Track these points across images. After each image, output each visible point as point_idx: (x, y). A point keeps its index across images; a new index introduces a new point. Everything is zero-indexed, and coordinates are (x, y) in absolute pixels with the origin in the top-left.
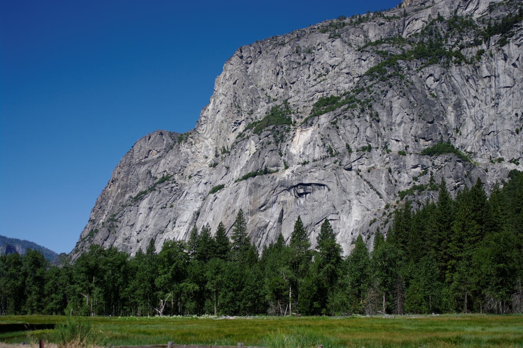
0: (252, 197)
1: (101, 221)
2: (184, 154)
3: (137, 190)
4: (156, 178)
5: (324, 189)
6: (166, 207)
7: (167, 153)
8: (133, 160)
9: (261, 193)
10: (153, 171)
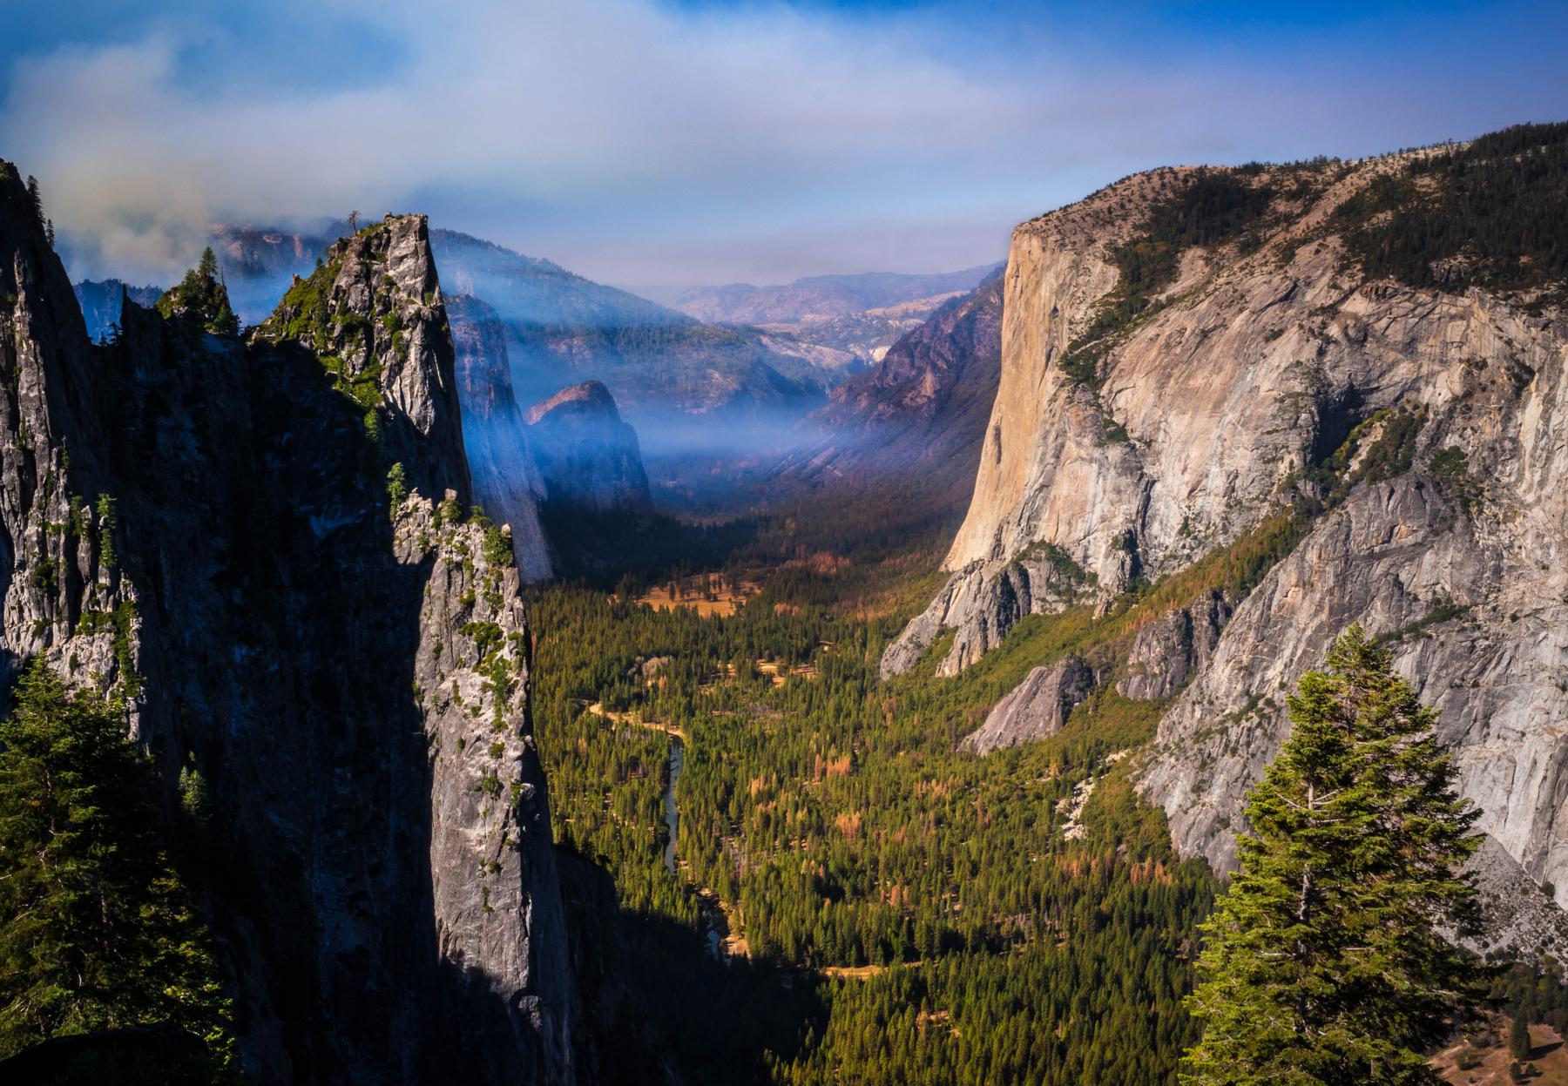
3: (1369, 620)
8: (1353, 546)
10: (1403, 577)
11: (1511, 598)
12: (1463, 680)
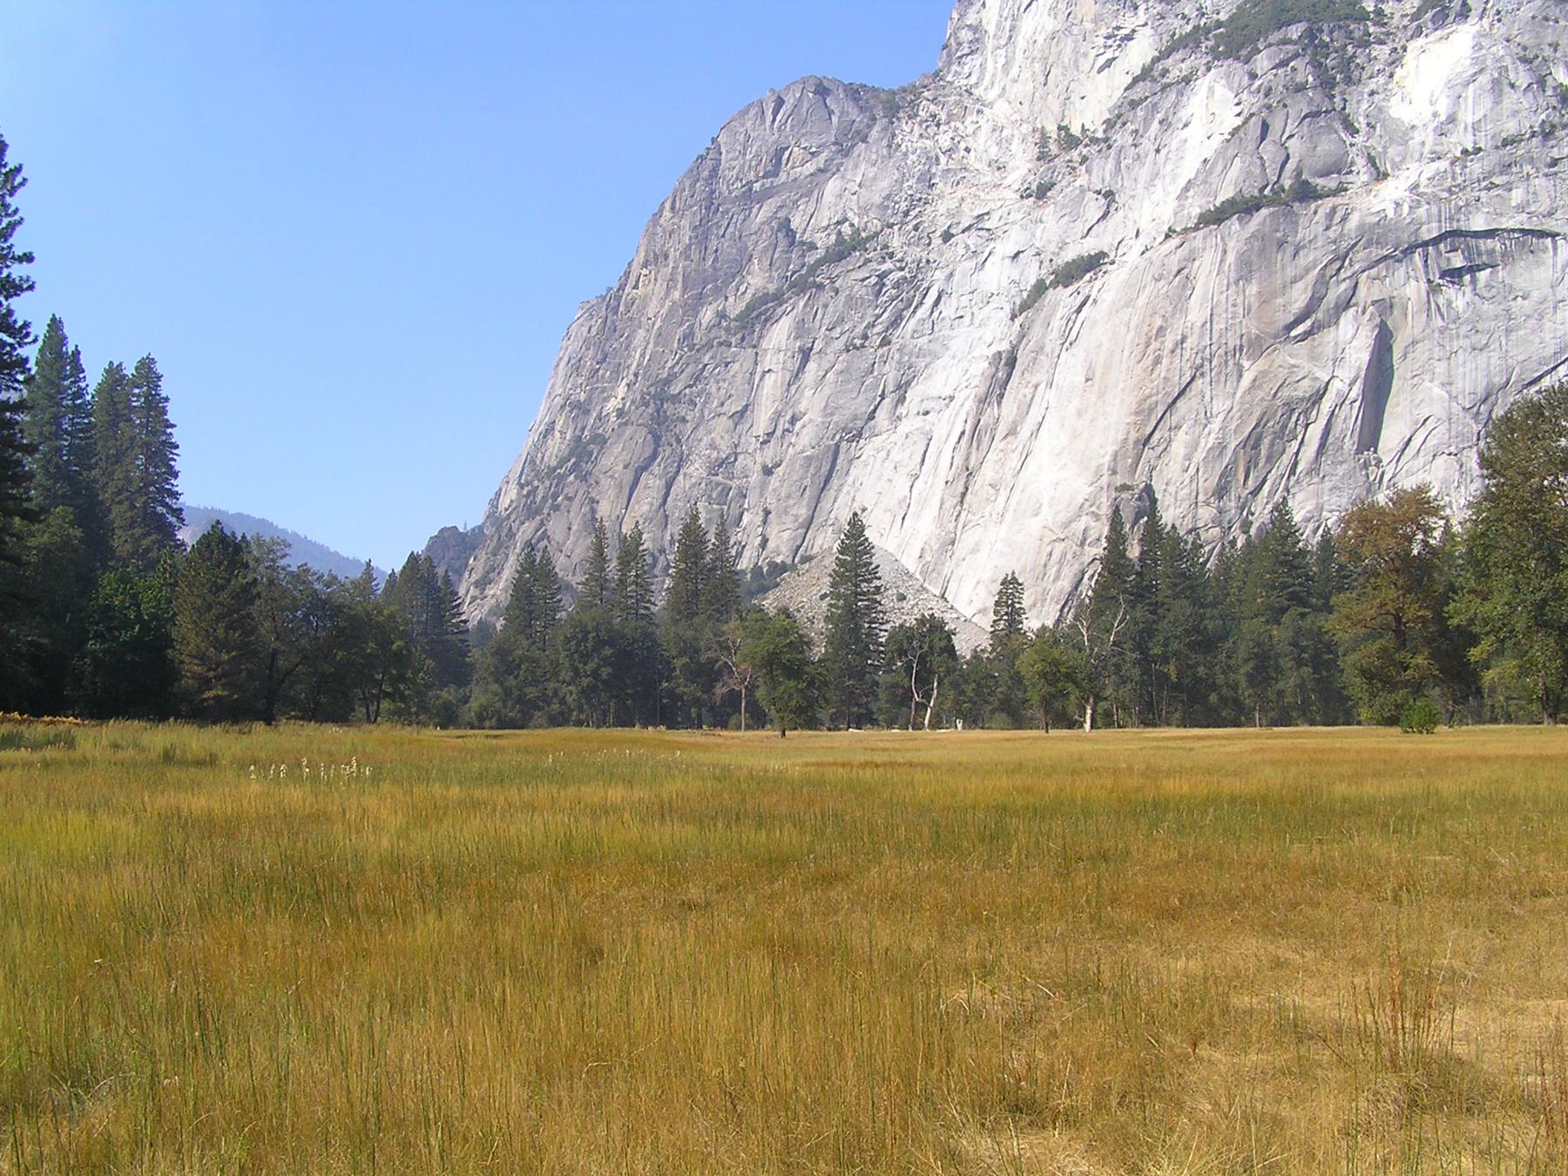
0: (1253, 289)
1: (612, 405)
2: (913, 157)
3: (742, 289)
4: (812, 247)
5: (1555, 249)
6: (863, 346)
7: (847, 155)
9: (1290, 272)
10: (796, 222)
11: (942, 209)
12: (865, 337)
